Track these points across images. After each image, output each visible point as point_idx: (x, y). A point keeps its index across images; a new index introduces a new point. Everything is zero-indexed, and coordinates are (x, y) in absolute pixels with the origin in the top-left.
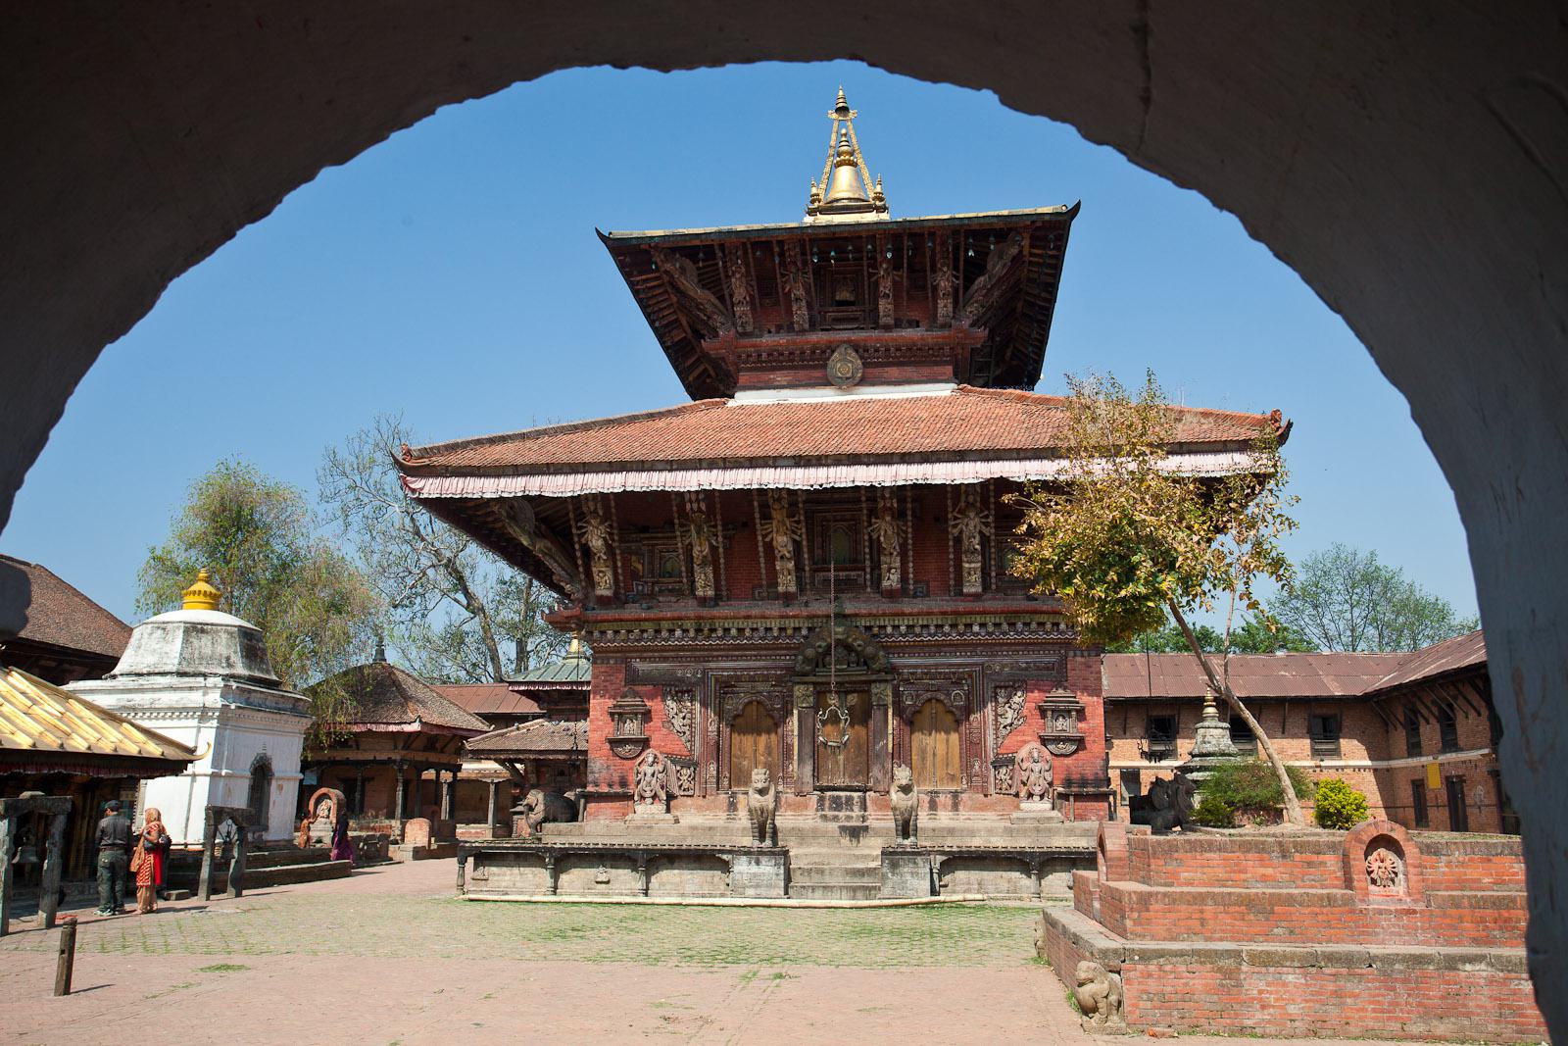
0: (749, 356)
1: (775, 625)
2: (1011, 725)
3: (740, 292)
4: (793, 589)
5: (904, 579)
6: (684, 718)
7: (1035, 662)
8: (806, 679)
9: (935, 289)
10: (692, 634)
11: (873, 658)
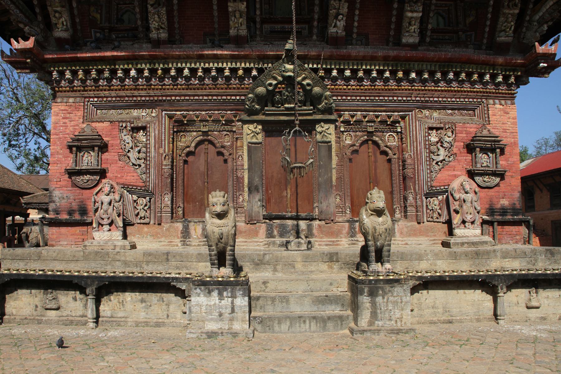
2: (441, 162)
5: (348, 28)
6: (139, 152)
8: (255, 118)
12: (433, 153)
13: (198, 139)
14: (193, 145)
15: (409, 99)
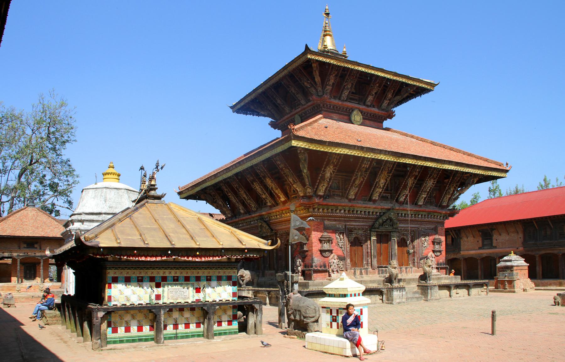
1: (371, 211)
4: (377, 199)
10: (347, 212)
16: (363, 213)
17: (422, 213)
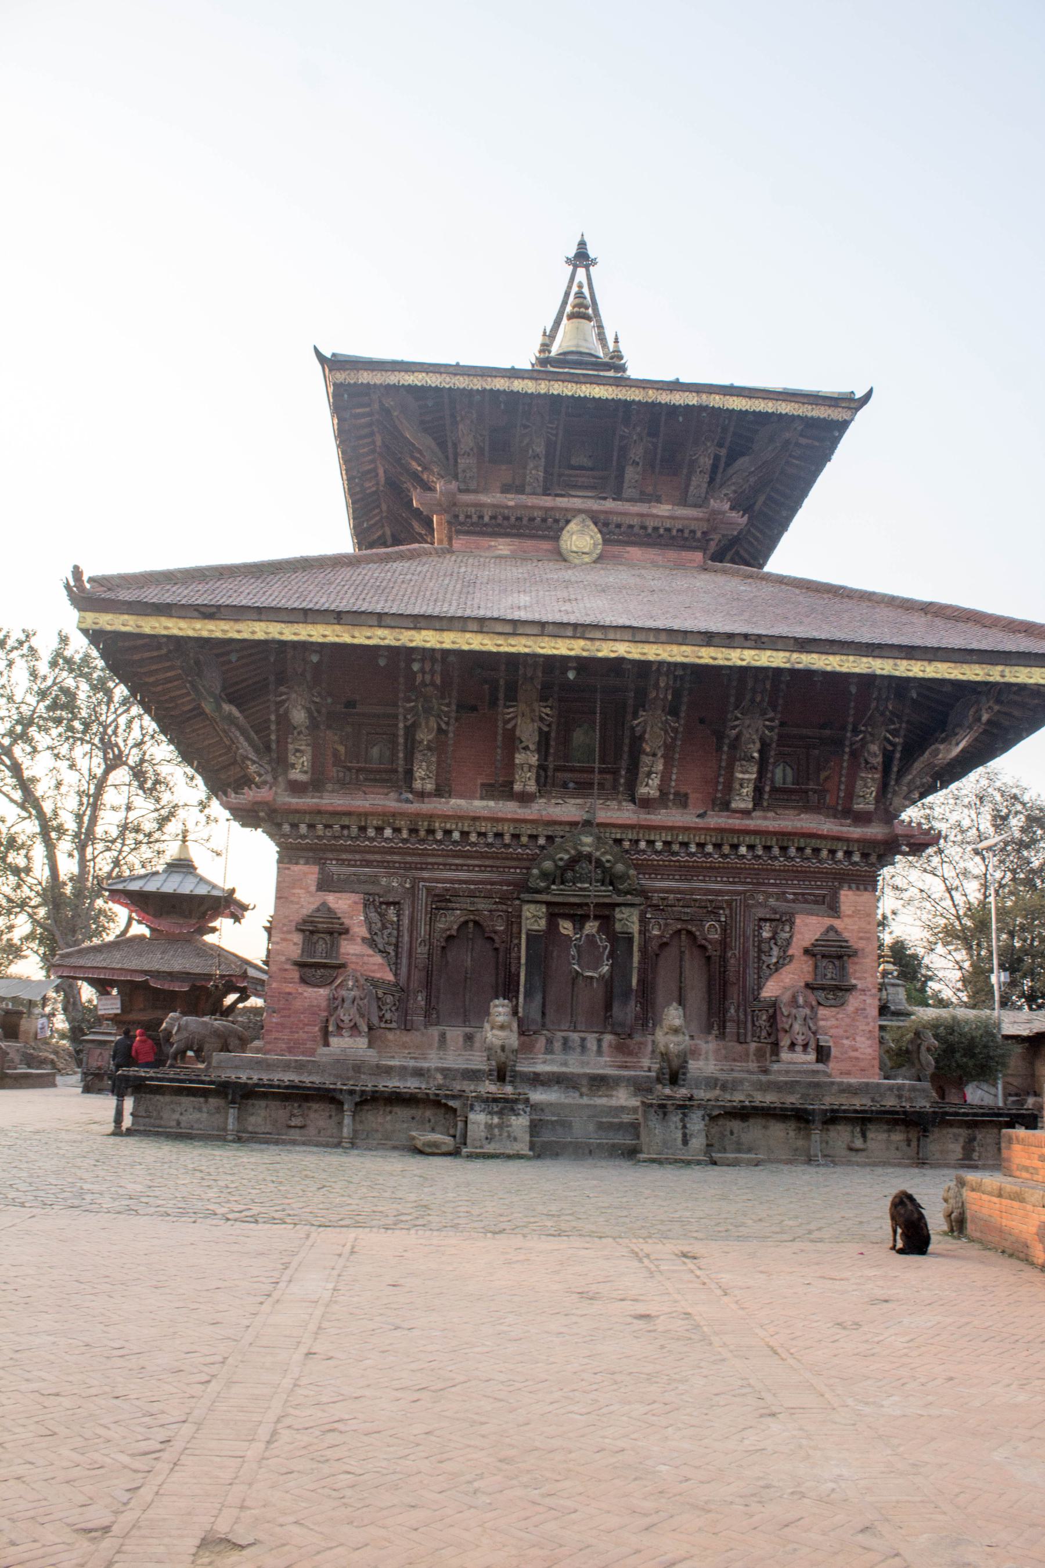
0: (468, 517)
1: (508, 829)
3: (467, 442)
4: (532, 787)
7: (803, 894)
9: (692, 464)
10: (405, 834)
11: (621, 877)
12: (764, 952)
13: (462, 919)
14: (455, 927)
15: (737, 880)
16: (473, 838)
17: (749, 840)
